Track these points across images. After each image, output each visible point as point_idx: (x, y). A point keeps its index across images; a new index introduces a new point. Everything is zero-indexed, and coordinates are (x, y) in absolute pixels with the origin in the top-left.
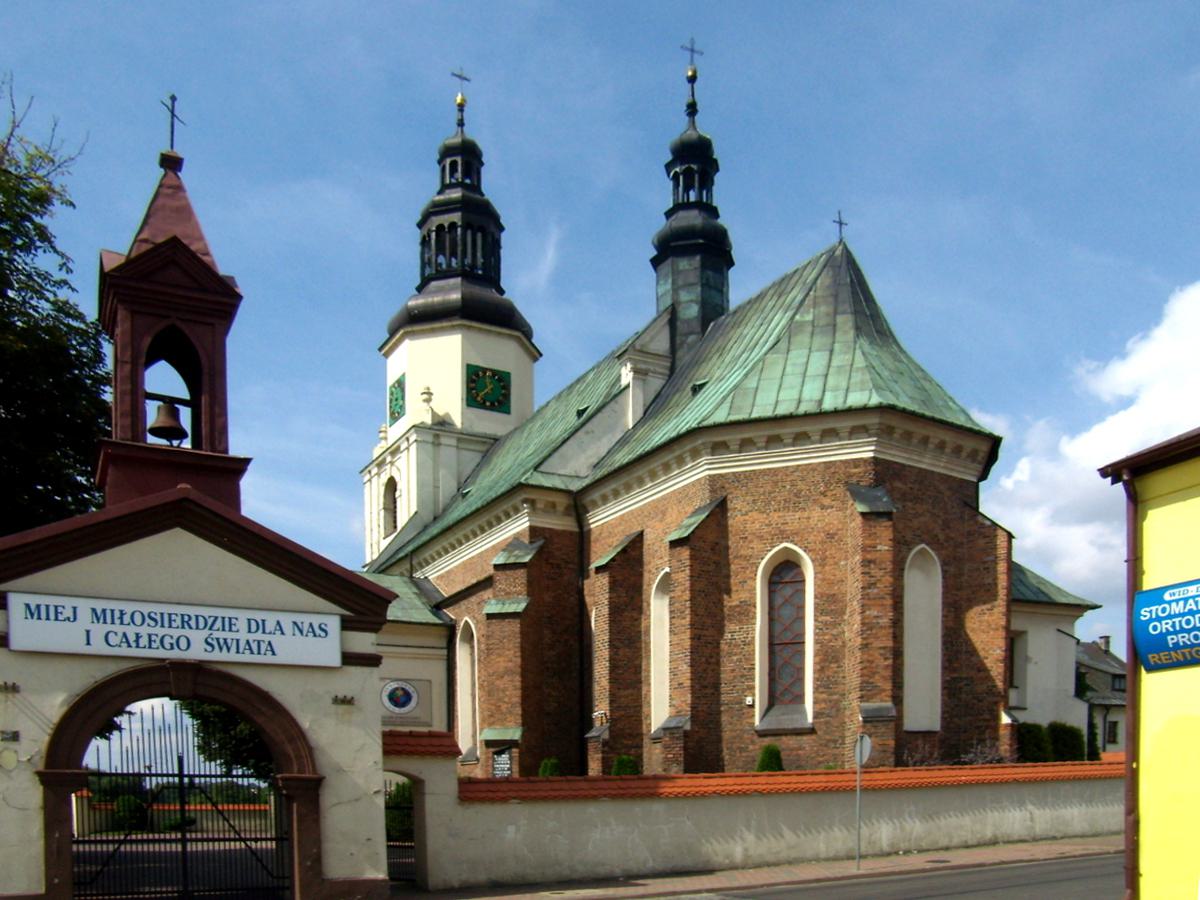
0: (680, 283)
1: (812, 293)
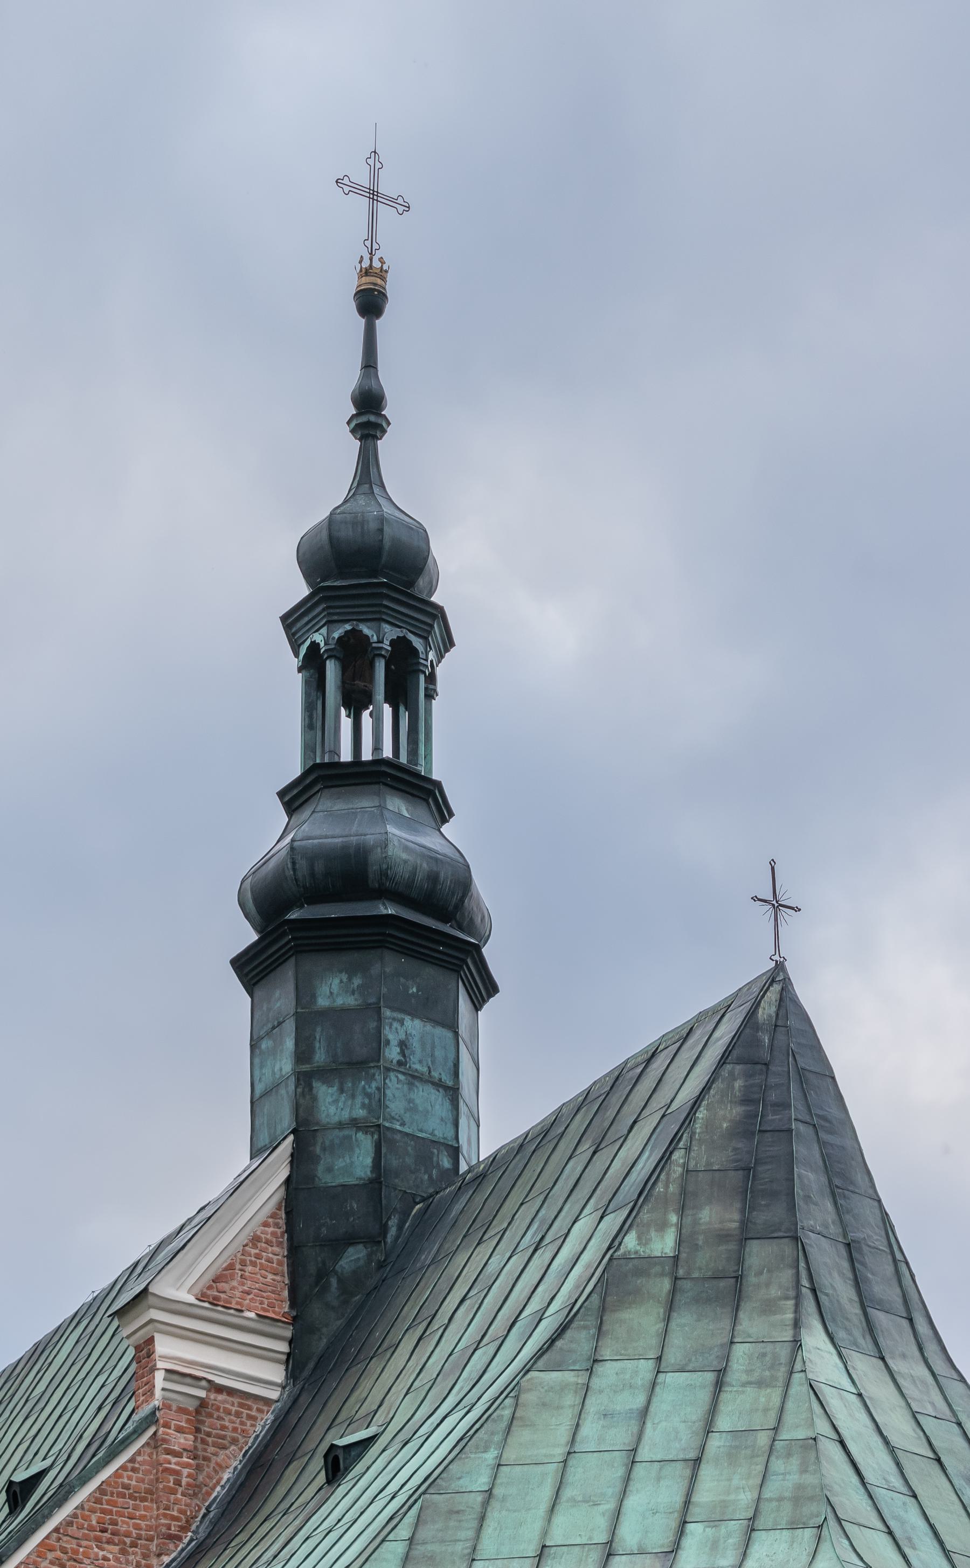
0: (320, 1057)
1: (678, 1156)
